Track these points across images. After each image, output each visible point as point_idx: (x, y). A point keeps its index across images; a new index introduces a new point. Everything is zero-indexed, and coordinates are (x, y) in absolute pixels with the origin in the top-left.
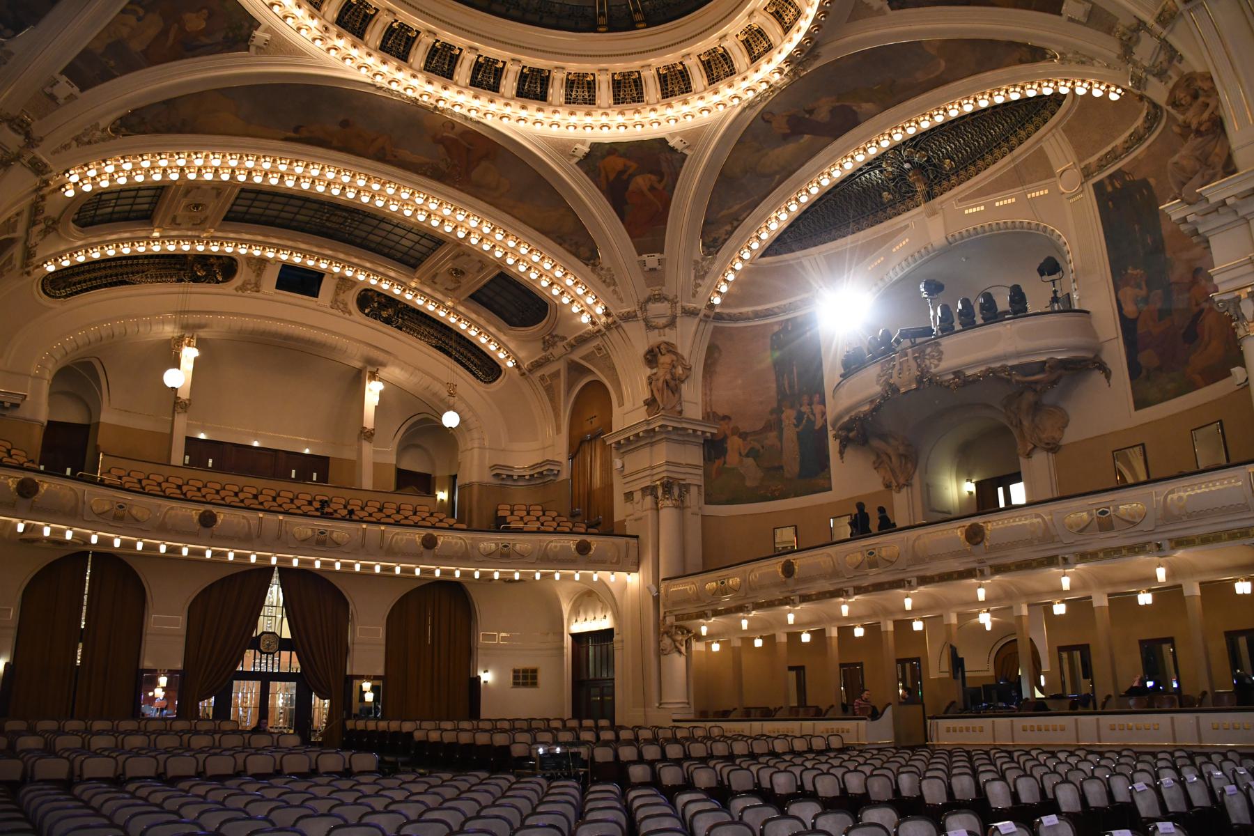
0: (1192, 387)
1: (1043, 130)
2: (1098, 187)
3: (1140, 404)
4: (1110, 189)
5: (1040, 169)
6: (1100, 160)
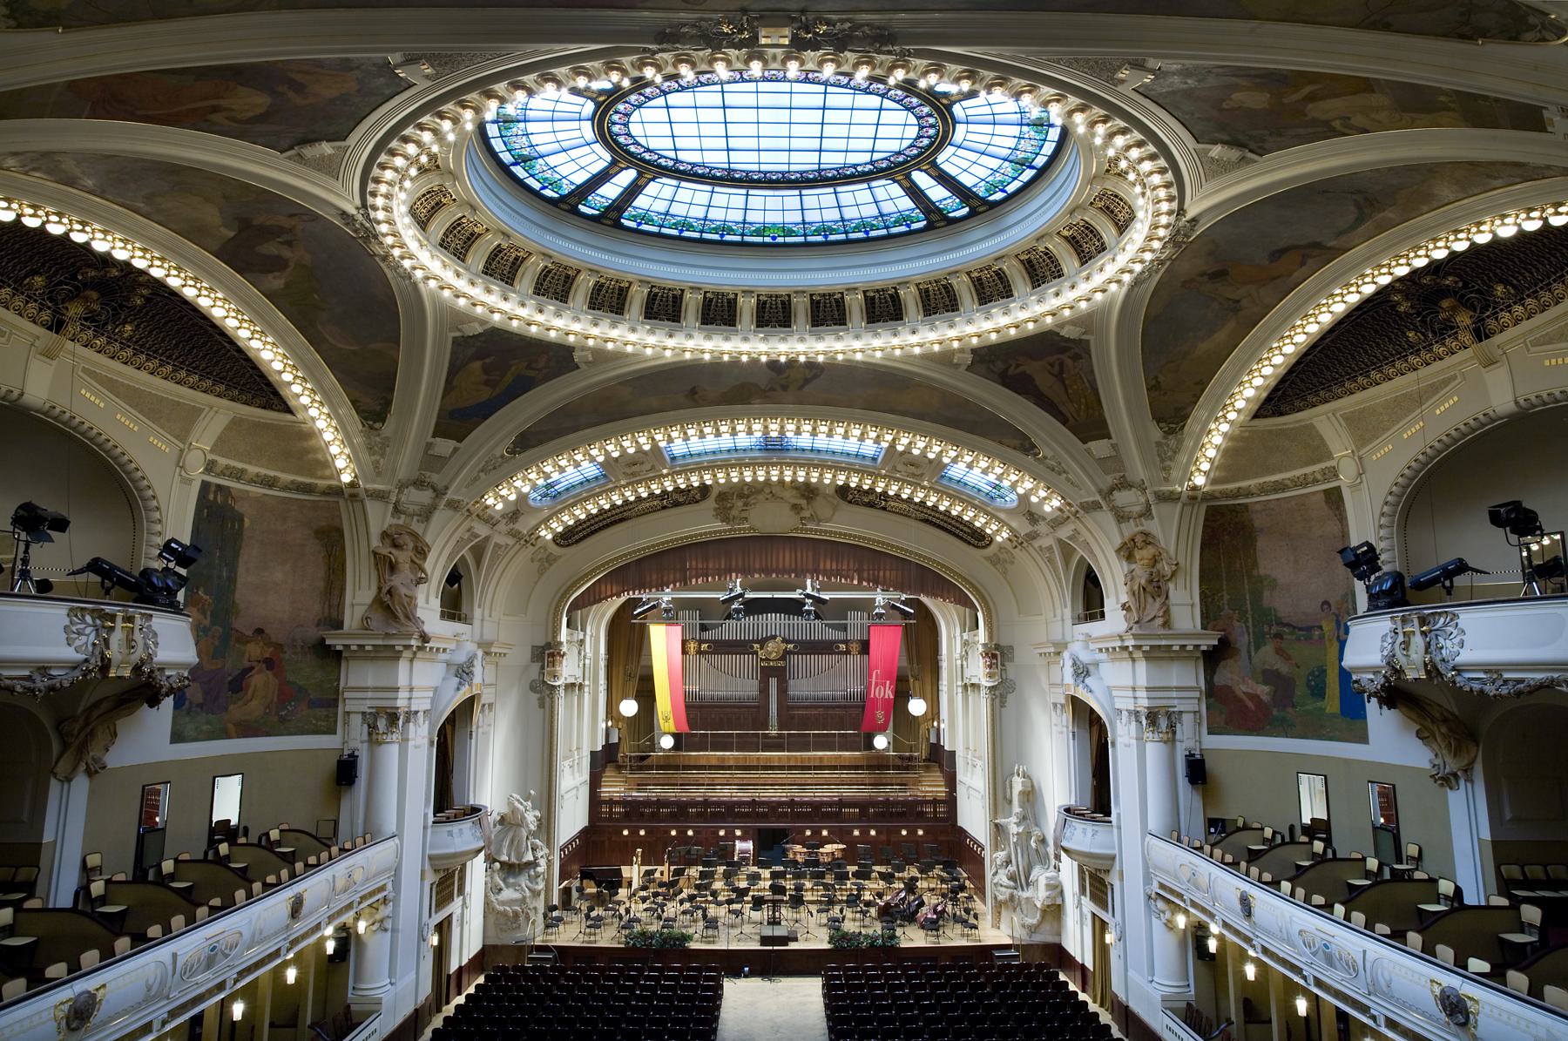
0: (224, 734)
1: (224, 402)
2: (205, 486)
3: (177, 737)
4: (211, 497)
5: (180, 422)
6: (227, 467)
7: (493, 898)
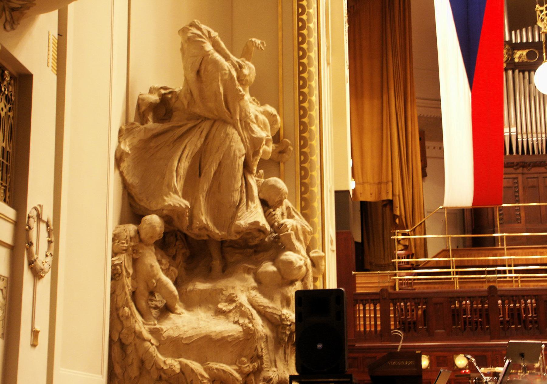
7: (141, 326)
